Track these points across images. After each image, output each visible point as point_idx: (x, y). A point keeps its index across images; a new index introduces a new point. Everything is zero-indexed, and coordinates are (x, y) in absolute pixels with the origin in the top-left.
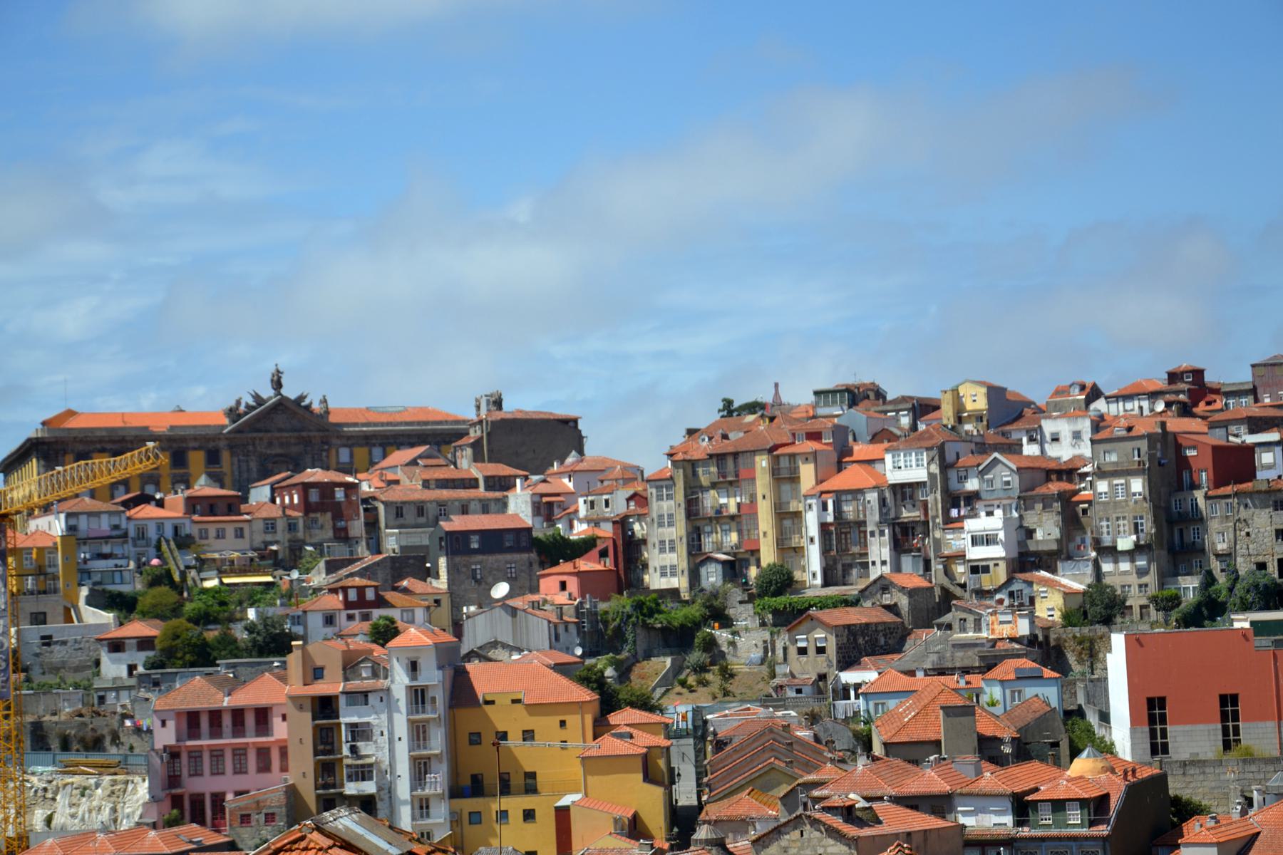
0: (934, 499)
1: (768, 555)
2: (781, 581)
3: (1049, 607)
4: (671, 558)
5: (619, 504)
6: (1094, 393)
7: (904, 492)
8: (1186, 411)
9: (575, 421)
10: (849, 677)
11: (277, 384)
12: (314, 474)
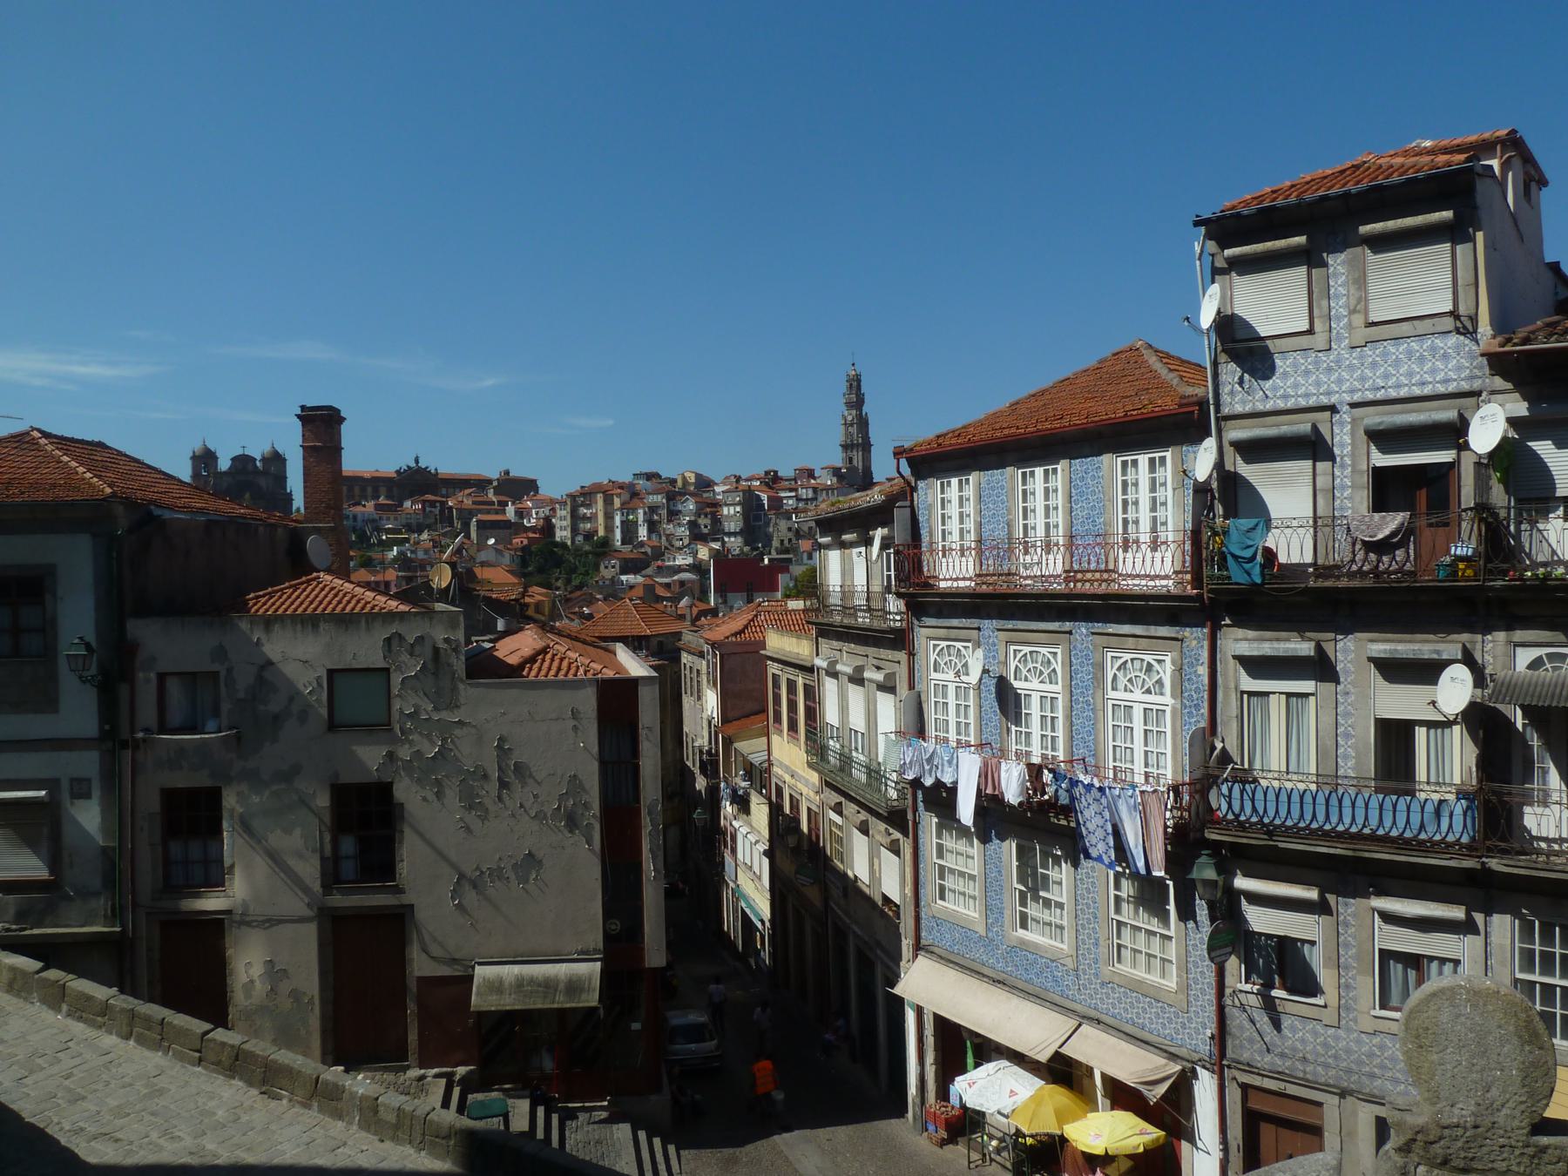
0: (664, 512)
1: (601, 533)
2: (606, 543)
3: (703, 553)
4: (564, 533)
5: (547, 511)
6: (738, 479)
7: (653, 509)
8: (767, 484)
9: (534, 482)
10: (624, 578)
11: (417, 461)
12: (429, 497)
